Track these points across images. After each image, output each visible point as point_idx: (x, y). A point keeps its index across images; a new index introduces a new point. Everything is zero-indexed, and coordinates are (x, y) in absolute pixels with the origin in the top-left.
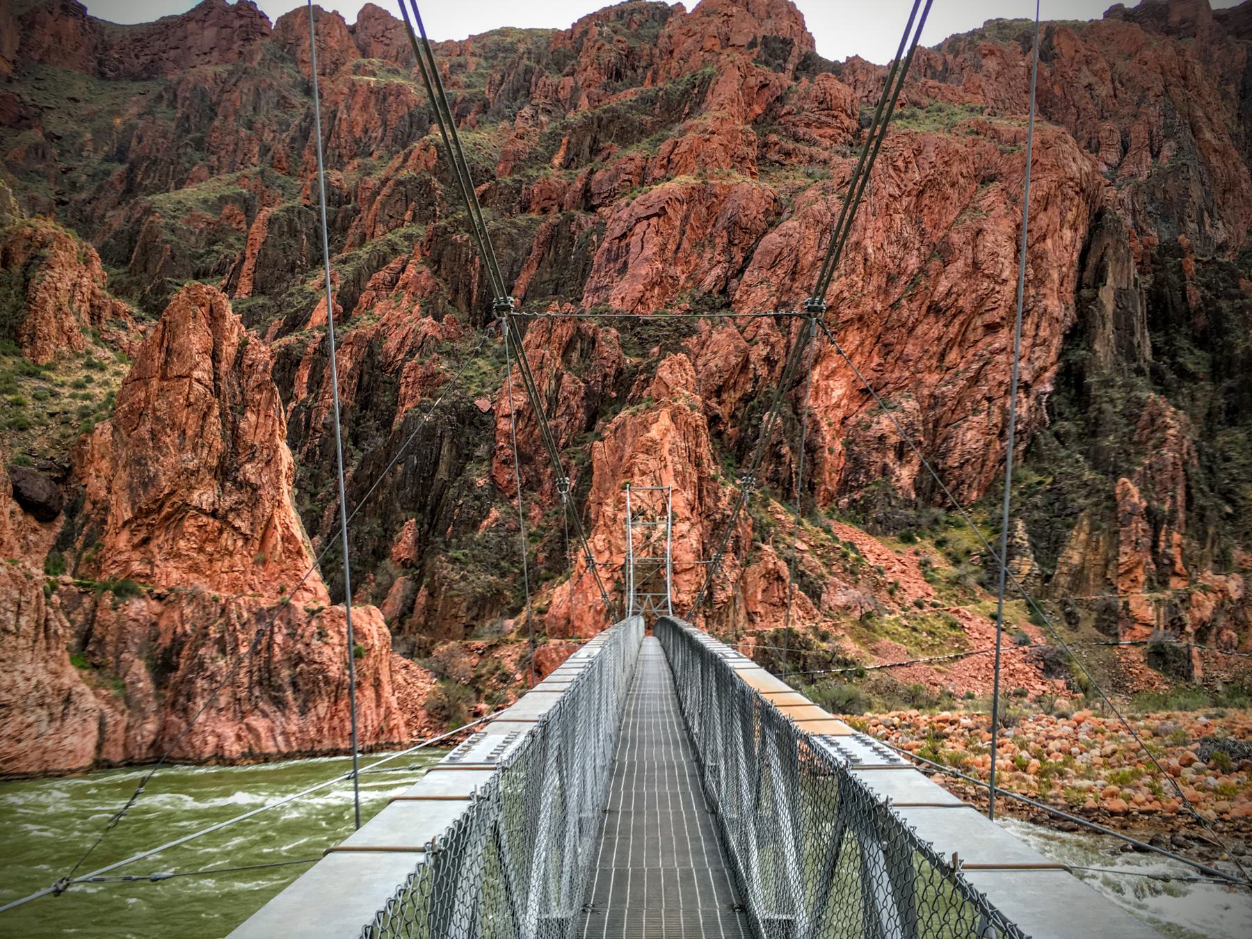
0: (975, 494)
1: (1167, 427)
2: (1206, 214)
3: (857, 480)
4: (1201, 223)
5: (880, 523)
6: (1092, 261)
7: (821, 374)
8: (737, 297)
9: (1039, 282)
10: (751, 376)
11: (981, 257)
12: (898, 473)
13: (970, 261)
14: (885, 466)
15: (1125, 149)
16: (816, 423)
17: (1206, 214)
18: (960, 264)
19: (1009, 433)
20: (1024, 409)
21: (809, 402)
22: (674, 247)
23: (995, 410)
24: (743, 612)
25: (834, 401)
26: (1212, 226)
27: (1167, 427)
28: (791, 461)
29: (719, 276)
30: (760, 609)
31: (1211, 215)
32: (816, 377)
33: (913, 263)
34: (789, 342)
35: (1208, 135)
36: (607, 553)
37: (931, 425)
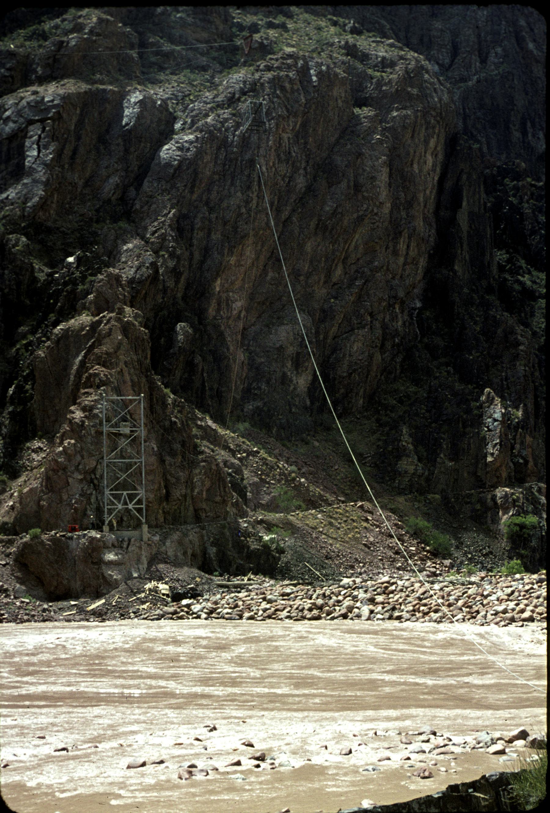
0: (361, 401)
1: (518, 344)
2: (529, 124)
3: (259, 388)
4: (524, 133)
5: (284, 429)
6: (449, 185)
7: (222, 285)
8: (138, 206)
9: (409, 205)
10: (161, 287)
11: (361, 180)
12: (295, 382)
13: (352, 184)
14: (284, 375)
15: (455, 52)
16: (221, 335)
17: (529, 124)
18: (343, 185)
19: (388, 345)
20: (400, 323)
21: (211, 312)
22: (70, 153)
23: (378, 325)
24: (191, 508)
25: (235, 312)
26: (534, 136)
27: (518, 344)
28: (203, 369)
29: (117, 185)
30: (204, 506)
31: (533, 126)
32: (218, 289)
33: (301, 182)
34: (192, 254)
35: (531, 46)
36: (78, 458)
37: (321, 337)
